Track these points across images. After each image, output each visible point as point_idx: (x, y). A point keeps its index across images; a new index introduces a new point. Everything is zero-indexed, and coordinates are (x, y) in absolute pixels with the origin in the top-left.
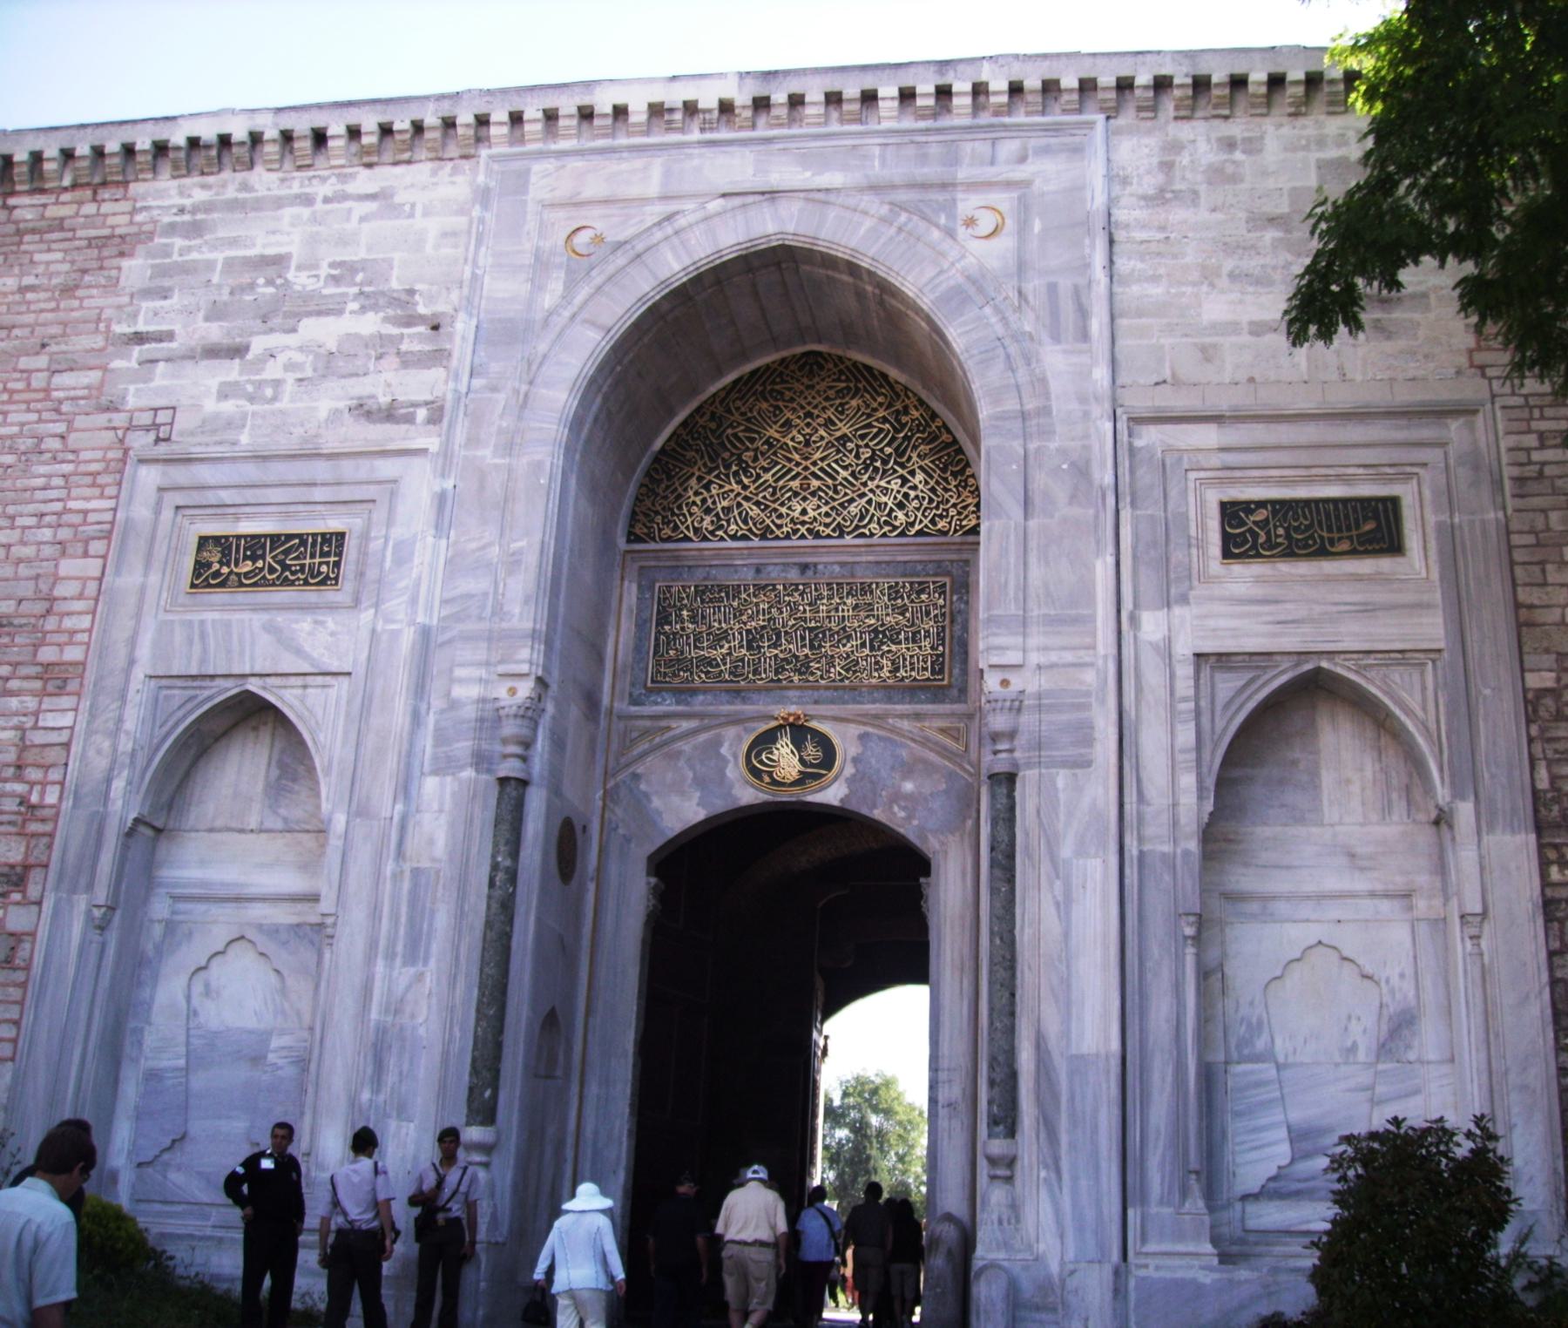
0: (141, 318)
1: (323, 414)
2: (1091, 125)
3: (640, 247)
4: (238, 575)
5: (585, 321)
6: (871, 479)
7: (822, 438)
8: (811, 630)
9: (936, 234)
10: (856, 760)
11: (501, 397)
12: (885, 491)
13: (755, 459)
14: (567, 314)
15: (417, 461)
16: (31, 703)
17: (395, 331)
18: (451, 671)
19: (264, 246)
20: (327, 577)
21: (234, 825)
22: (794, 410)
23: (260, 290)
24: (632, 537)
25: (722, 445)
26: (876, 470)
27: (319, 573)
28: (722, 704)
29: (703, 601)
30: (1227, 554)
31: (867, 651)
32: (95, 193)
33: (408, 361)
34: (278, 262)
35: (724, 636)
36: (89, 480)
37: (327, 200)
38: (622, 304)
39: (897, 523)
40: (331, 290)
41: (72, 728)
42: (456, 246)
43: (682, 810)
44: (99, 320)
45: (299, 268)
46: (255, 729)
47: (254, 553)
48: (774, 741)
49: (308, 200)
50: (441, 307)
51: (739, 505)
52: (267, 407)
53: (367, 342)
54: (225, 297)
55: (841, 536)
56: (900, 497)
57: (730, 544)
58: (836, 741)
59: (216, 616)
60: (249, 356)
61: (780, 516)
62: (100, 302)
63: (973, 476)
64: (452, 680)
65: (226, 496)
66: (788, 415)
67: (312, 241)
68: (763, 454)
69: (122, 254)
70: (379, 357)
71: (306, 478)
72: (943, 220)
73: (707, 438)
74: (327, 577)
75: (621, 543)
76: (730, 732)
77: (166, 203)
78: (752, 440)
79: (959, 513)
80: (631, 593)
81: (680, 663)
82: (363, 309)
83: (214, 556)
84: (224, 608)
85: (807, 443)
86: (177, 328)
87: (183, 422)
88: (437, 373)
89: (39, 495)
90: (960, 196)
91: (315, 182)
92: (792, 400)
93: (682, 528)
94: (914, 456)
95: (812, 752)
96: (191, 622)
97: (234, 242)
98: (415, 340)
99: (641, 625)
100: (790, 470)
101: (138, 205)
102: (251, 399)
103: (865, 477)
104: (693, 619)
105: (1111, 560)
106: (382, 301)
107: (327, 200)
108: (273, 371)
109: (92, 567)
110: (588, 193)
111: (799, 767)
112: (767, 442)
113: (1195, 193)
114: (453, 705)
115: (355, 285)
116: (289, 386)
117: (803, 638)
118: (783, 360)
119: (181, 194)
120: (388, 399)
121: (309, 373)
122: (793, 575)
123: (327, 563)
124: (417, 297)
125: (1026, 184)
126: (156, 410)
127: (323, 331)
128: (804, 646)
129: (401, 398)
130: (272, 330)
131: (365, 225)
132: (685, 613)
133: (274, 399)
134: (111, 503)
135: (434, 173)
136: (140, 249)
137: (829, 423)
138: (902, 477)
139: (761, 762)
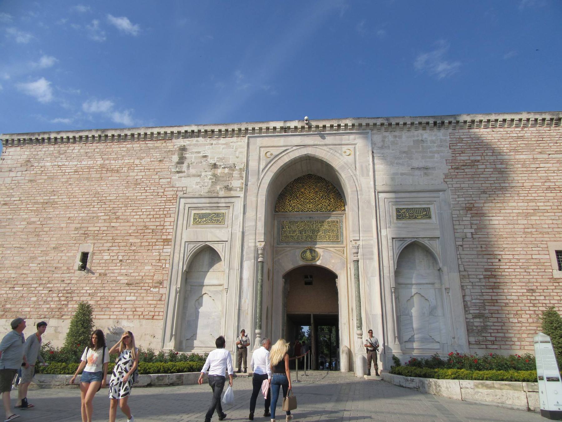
2: (368, 133)
9: (338, 155)
16: (161, 247)
24: (276, 211)
30: (397, 218)
35: (295, 231)
37: (215, 144)
43: (289, 266)
48: (306, 252)
53: (226, 174)
69: (172, 154)
72: (340, 152)
75: (274, 213)
76: (298, 250)
80: (276, 222)
81: (287, 237)
82: (224, 168)
87: (189, 190)
89: (159, 204)
99: (278, 229)
105: (375, 220)
107: (215, 144)
113: (389, 146)
119: (184, 142)
122: (308, 219)
125: (355, 144)
131: (224, 150)
137: (314, 188)
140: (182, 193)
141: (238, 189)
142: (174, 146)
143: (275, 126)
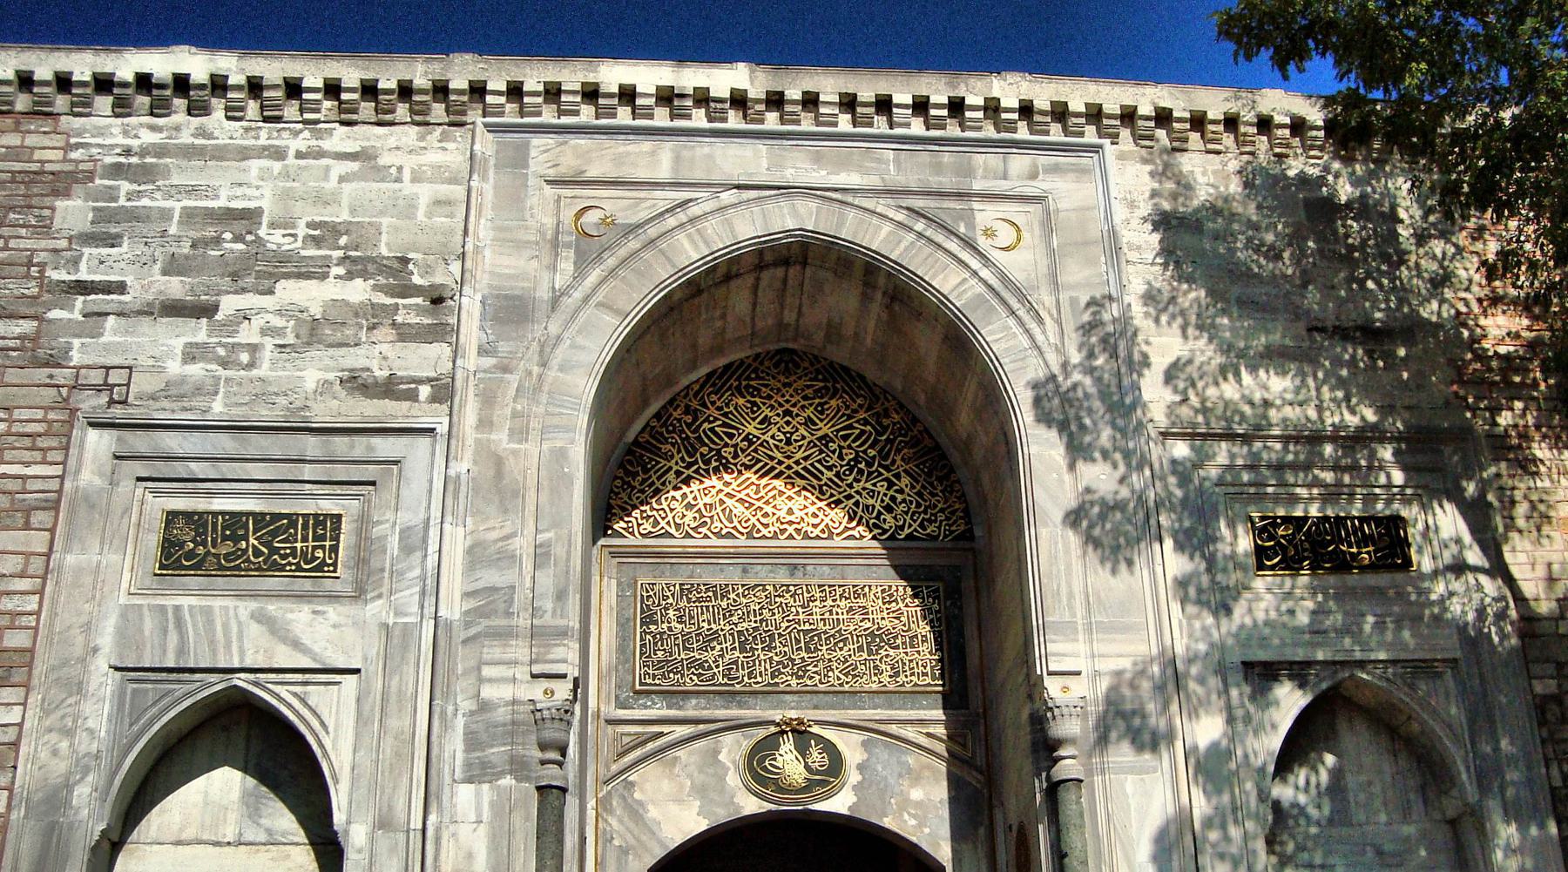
0: (83, 266)
1: (310, 385)
3: (652, 232)
4: (217, 556)
5: (599, 305)
6: (858, 481)
7: (804, 438)
8: (806, 632)
10: (861, 768)
11: (513, 379)
12: (872, 494)
13: (736, 456)
14: (578, 295)
15: (424, 442)
17: (389, 301)
18: (479, 669)
19: (230, 199)
20: (323, 563)
21: (205, 837)
22: (772, 407)
23: (227, 245)
25: (699, 438)
26: (861, 472)
27: (314, 558)
28: (717, 708)
29: (689, 600)
31: (865, 656)
32: (18, 123)
33: (405, 334)
34: (250, 216)
36: (27, 442)
38: (639, 294)
39: (886, 527)
40: (312, 252)
41: (20, 725)
42: (451, 216)
44: (30, 264)
45: (272, 225)
46: (226, 729)
47: (234, 533)
49: (279, 154)
50: (439, 279)
51: (722, 502)
52: (242, 372)
53: (357, 311)
54: (186, 249)
55: (830, 537)
56: (887, 500)
57: (715, 541)
58: (841, 747)
59: (193, 601)
60: (219, 316)
61: (766, 515)
62: (29, 244)
63: (958, 481)
64: (481, 680)
65: (198, 469)
66: (767, 412)
67: (285, 196)
68: (743, 451)
69: (56, 193)
70: (372, 328)
71: (294, 454)
72: (962, 229)
73: (683, 431)
74: (323, 563)
76: (728, 739)
77: (108, 142)
78: (731, 436)
79: (947, 519)
82: (350, 276)
83: (187, 536)
84: (202, 592)
85: (788, 443)
86: (129, 280)
87: (141, 384)
88: (441, 350)
90: (976, 206)
91: (285, 134)
92: (769, 397)
93: (663, 524)
94: (898, 458)
95: (816, 757)
96: (163, 608)
97: (192, 191)
98: (411, 312)
99: (623, 625)
100: (773, 468)
101: (73, 141)
102: (225, 364)
103: (851, 479)
104: (680, 620)
106: (371, 268)
107: (300, 155)
108: (248, 334)
109: (38, 541)
110: (593, 172)
111: (805, 774)
112: (746, 439)
114: (484, 706)
115: (339, 248)
116: (268, 353)
117: (798, 641)
118: (758, 355)
119: (126, 133)
120: (386, 373)
121: (290, 339)
123: (323, 547)
124: (411, 266)
126: (108, 368)
127: (311, 295)
128: (799, 649)
129: (399, 374)
130: (244, 290)
131: (347, 187)
132: (671, 612)
133: (251, 365)
134: (58, 470)
135: (422, 138)
136: (77, 189)
137: (809, 422)
138: (886, 479)
139: (765, 769)
140: (104, 399)
141: (425, 391)
142: (69, 148)
143: (627, 81)
